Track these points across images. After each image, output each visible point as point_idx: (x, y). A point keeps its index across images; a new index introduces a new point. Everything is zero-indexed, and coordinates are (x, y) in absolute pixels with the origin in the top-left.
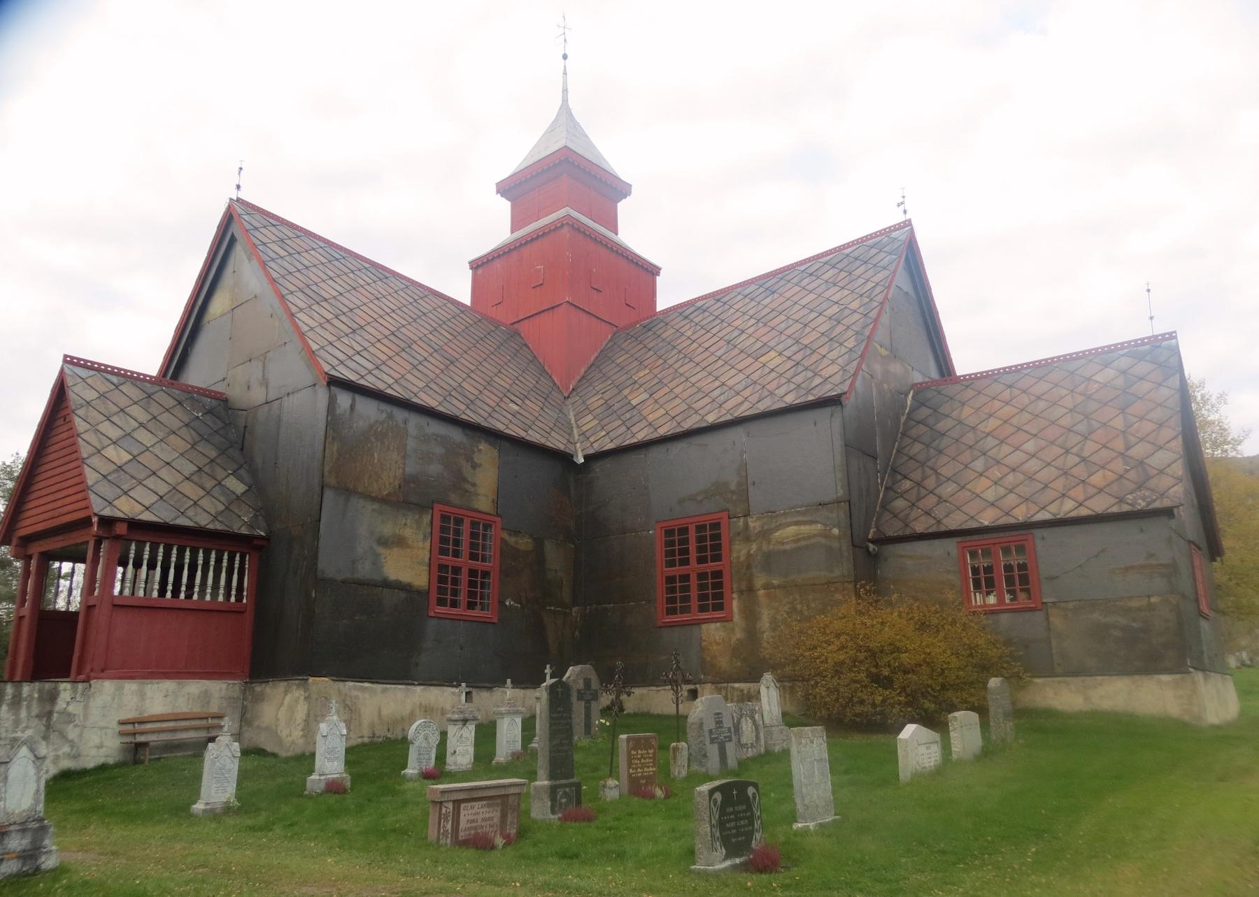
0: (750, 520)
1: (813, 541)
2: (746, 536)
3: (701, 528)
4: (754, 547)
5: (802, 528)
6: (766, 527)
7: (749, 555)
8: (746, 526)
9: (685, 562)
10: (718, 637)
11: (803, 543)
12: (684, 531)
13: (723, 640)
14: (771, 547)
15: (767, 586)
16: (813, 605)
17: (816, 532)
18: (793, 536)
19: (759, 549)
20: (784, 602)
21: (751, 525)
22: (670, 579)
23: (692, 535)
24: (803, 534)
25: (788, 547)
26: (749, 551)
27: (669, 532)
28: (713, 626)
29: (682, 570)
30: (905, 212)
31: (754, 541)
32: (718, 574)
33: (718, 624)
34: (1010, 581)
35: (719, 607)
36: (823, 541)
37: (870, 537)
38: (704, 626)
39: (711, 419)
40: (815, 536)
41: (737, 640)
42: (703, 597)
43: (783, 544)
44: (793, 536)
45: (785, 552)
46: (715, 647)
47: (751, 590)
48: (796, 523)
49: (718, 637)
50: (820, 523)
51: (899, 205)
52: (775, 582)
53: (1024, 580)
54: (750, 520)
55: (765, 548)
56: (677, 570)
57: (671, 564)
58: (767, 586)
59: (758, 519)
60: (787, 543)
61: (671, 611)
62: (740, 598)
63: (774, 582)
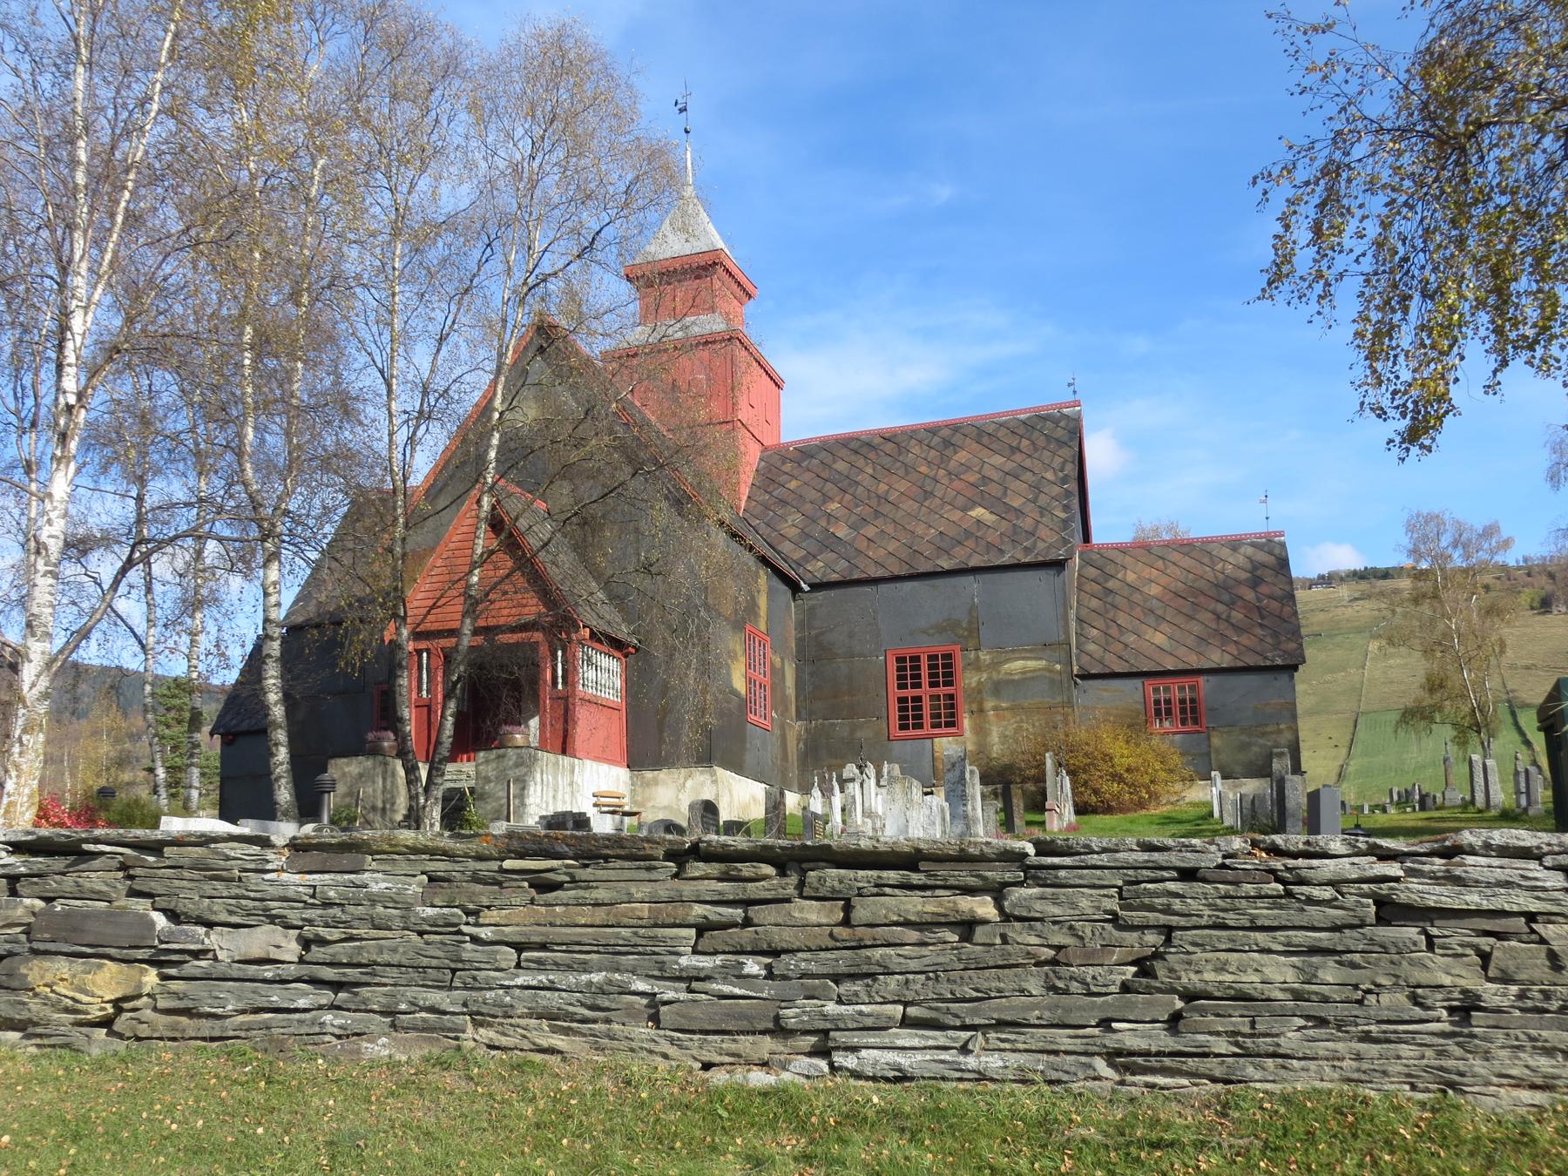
1: (1038, 673)
2: (977, 666)
3: (932, 657)
4: (985, 676)
7: (979, 683)
8: (978, 658)
9: (919, 686)
11: (1029, 675)
12: (916, 659)
15: (995, 709)
16: (1037, 724)
22: (902, 700)
23: (924, 664)
25: (1016, 677)
27: (900, 660)
30: (1075, 392)
32: (951, 697)
34: (1183, 711)
35: (948, 725)
37: (1075, 672)
38: (936, 740)
39: (946, 564)
45: (1013, 680)
47: (981, 710)
48: (1023, 659)
51: (1069, 385)
53: (1193, 710)
55: (995, 676)
56: (909, 692)
57: (901, 687)
58: (995, 709)
61: (903, 727)
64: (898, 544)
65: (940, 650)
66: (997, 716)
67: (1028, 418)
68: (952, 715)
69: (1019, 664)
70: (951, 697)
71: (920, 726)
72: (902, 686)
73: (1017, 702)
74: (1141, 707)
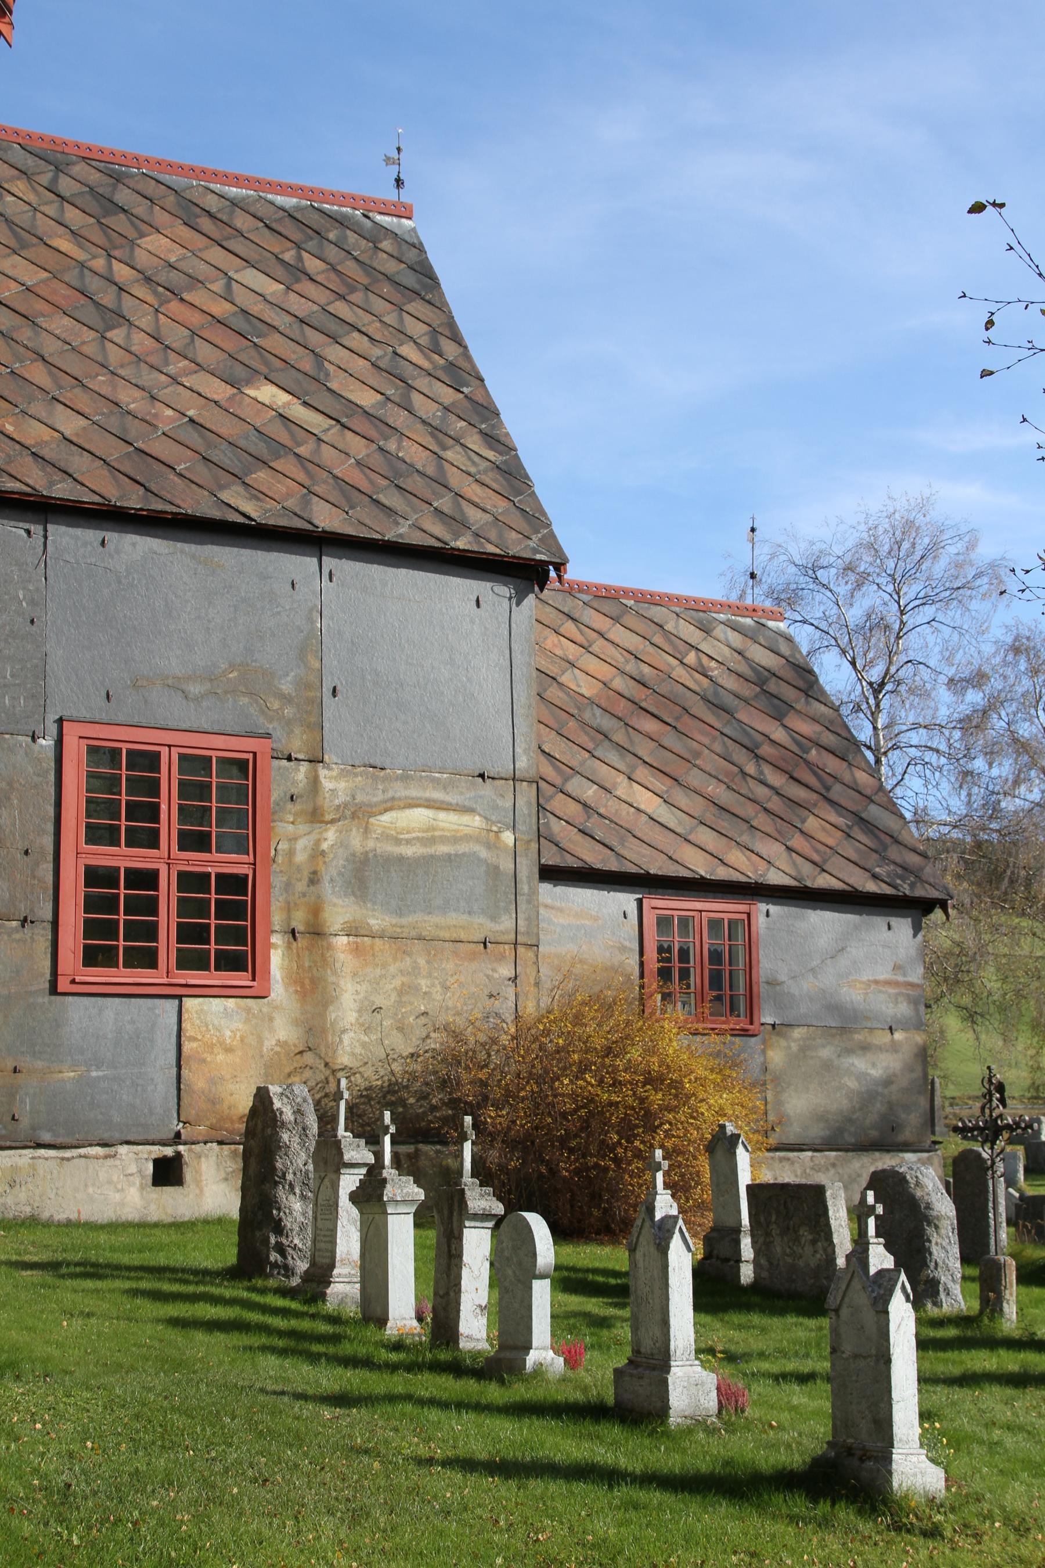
0: (323, 773)
1: (462, 848)
5: (442, 815)
6: (359, 798)
7: (317, 854)
8: (315, 782)
10: (228, 1033)
11: (443, 849)
12: (151, 760)
13: (242, 1040)
14: (370, 844)
15: (353, 931)
17: (467, 831)
18: (421, 830)
19: (342, 844)
20: (392, 969)
21: (327, 784)
24: (443, 830)
25: (409, 851)
26: (318, 843)
28: (216, 1004)
29: (196, 861)
30: (399, 182)
31: (332, 822)
33: (231, 1003)
36: (484, 853)
38: (188, 1003)
40: (467, 838)
41: (279, 1042)
42: (186, 933)
43: (398, 842)
44: (424, 831)
45: (401, 859)
46: (220, 1057)
47: (317, 932)
48: (430, 804)
49: (228, 1033)
50: (480, 815)
52: (375, 923)
54: (323, 773)
55: (356, 842)
57: (96, 835)
59: (343, 774)
60: (408, 842)
61: (92, 957)
62: (289, 947)
63: (372, 922)
64: (83, 422)
65: (218, 746)
66: (357, 950)
67: (298, 208)
68: (239, 936)
69: (419, 816)
70: (234, 883)
71: (148, 959)
72: (96, 835)
73: (404, 921)
74: (632, 962)
